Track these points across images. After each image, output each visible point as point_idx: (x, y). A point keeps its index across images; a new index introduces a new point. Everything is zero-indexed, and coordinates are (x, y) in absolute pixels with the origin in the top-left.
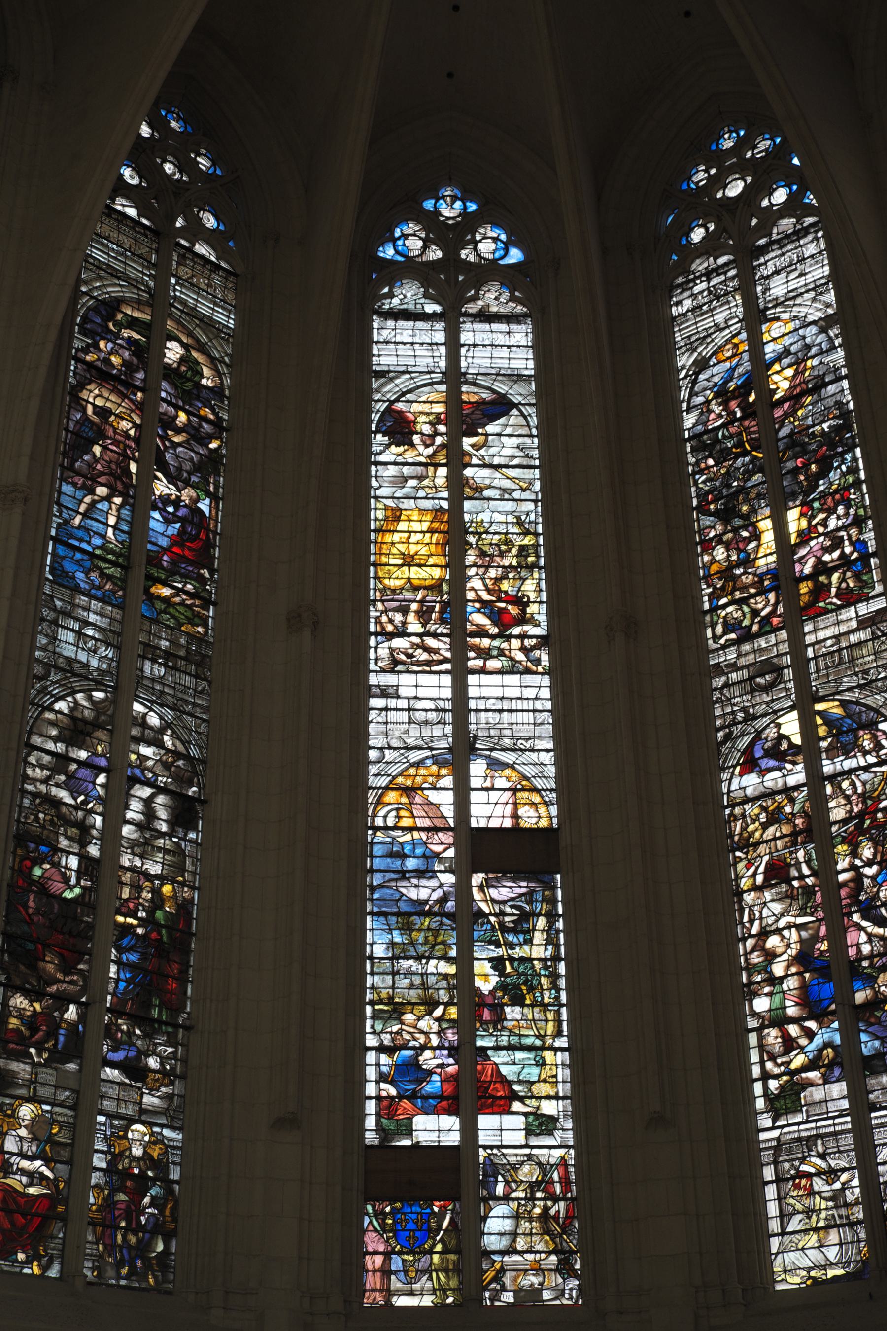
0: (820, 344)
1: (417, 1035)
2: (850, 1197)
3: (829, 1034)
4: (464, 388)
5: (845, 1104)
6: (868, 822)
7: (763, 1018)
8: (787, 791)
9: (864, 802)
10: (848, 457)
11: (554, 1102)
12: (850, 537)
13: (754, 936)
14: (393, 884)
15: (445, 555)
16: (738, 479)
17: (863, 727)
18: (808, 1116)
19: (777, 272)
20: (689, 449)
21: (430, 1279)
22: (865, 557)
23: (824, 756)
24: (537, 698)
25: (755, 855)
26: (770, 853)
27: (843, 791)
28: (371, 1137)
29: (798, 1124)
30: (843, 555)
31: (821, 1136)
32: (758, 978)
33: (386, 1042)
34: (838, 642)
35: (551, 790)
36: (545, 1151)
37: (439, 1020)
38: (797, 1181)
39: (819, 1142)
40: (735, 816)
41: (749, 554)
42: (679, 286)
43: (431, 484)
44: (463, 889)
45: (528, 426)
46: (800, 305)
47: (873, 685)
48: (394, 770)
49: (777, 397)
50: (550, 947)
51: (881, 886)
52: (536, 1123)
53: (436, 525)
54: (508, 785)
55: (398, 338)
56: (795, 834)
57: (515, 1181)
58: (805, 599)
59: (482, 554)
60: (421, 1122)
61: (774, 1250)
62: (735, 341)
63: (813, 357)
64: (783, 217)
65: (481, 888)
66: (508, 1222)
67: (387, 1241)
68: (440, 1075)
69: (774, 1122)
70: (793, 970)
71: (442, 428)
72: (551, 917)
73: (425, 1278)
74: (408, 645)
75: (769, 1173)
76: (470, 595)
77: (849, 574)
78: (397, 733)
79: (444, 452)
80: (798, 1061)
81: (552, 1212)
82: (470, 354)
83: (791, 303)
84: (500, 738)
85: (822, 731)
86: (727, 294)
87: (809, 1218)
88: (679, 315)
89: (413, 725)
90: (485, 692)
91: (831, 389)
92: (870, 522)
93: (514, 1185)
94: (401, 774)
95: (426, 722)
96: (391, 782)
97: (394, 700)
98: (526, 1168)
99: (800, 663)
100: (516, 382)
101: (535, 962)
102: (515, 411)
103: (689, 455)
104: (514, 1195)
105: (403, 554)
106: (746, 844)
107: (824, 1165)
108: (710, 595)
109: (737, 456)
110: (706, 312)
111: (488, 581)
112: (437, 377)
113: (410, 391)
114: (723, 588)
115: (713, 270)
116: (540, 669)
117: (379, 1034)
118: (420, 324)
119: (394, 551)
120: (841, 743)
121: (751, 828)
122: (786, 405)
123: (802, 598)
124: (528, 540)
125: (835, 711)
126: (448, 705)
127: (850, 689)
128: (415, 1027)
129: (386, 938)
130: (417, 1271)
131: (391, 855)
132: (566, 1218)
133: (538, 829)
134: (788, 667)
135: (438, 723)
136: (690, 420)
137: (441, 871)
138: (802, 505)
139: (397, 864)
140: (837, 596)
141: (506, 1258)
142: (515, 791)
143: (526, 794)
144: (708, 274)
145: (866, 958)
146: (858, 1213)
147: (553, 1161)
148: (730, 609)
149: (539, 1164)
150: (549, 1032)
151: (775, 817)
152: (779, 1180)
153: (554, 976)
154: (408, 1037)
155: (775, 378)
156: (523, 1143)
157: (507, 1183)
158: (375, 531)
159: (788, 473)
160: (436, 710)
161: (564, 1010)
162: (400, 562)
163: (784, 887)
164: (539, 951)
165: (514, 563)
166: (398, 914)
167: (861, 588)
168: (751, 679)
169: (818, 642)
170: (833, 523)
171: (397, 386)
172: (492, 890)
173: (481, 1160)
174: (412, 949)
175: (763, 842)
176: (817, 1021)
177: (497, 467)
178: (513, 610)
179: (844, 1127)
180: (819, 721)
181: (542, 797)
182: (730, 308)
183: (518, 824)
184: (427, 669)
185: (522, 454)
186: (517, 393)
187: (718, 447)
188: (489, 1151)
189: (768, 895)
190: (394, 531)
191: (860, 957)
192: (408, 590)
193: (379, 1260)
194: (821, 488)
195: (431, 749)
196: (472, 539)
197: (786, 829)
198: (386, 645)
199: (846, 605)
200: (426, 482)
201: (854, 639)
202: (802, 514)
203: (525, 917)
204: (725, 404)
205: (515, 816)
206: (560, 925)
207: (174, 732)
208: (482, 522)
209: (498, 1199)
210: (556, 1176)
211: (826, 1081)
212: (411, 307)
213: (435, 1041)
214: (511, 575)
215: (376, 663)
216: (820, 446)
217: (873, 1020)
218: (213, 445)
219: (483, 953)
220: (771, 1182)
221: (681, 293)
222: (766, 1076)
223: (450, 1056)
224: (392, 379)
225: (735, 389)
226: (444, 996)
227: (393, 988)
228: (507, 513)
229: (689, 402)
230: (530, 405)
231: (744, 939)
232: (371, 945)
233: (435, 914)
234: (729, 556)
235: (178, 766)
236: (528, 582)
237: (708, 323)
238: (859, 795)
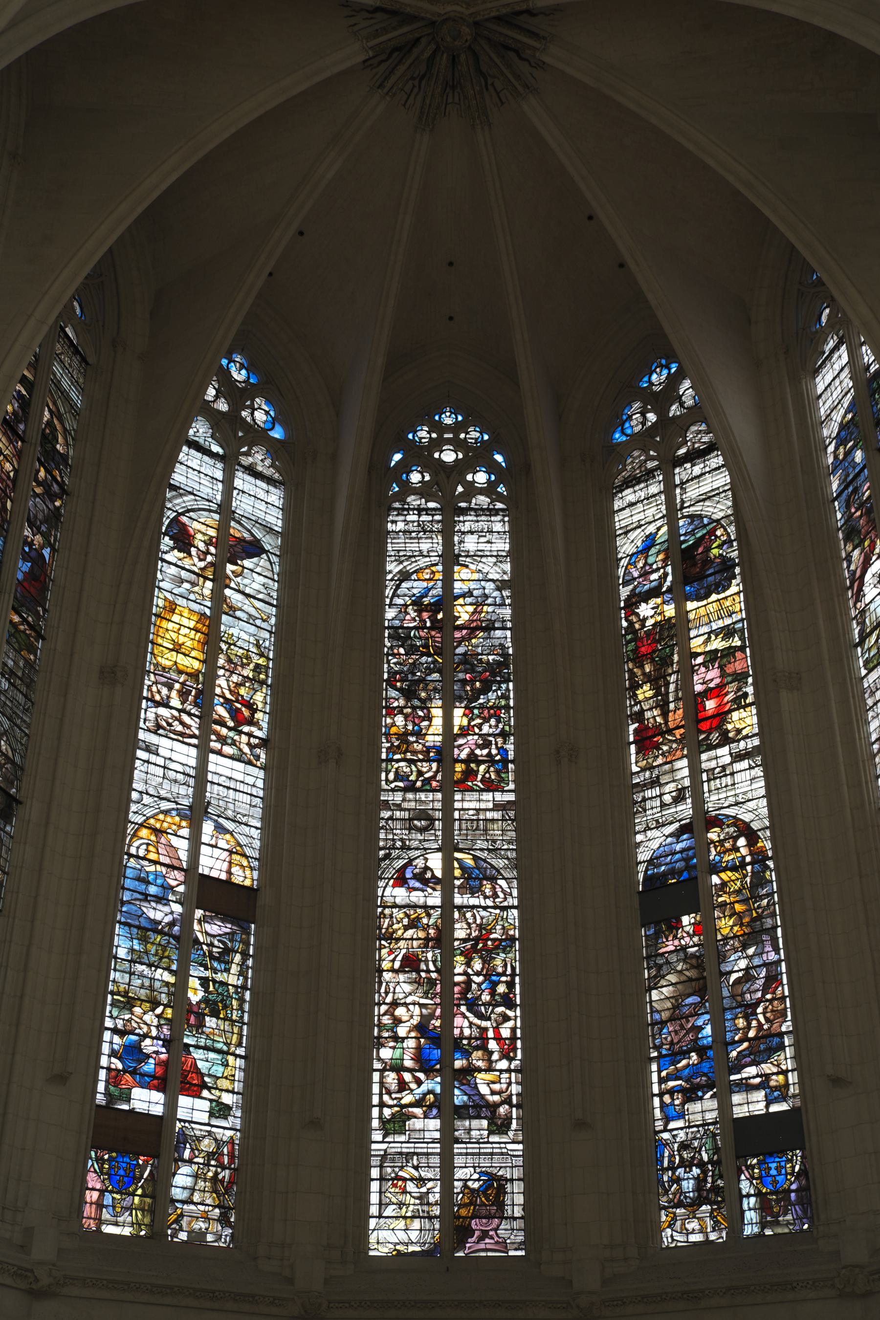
1: (142, 1026)
2: (432, 1199)
3: (434, 1084)
4: (233, 524)
5: (437, 1135)
6: (481, 945)
7: (386, 1063)
8: (425, 907)
9: (480, 931)
10: (504, 686)
11: (231, 1095)
12: (496, 744)
13: (387, 1004)
14: (138, 903)
15: (203, 653)
16: (421, 672)
17: (487, 879)
18: (409, 1138)
19: (472, 533)
20: (386, 635)
21: (131, 1215)
22: (505, 761)
23: (456, 890)
24: (254, 786)
25: (396, 946)
26: (408, 948)
27: (466, 920)
28: (100, 1099)
29: (402, 1143)
30: (490, 753)
31: (418, 1154)
32: (386, 1034)
33: (119, 1026)
34: (478, 814)
35: (255, 859)
36: (221, 1130)
37: (159, 1016)
39: (415, 1158)
40: (385, 915)
41: (422, 729)
43: (200, 592)
44: (186, 920)
45: (272, 571)
48: (149, 812)
49: (458, 623)
50: (241, 978)
51: (483, 991)
52: (217, 1109)
53: (199, 626)
54: (227, 847)
55: (189, 463)
56: (427, 939)
57: (198, 1150)
58: (458, 776)
59: (229, 661)
60: (138, 1093)
61: (372, 1227)
62: (433, 569)
63: (489, 605)
64: (481, 494)
65: (200, 921)
66: (190, 1179)
67: (103, 1182)
68: (155, 1059)
69: (384, 1137)
70: (413, 1034)
71: (212, 550)
72: (245, 955)
73: (127, 1213)
74: (169, 716)
75: (375, 1173)
76: (218, 691)
77: (492, 769)
78: (154, 783)
79: (212, 569)
80: (407, 1099)
81: (220, 1177)
82: (239, 498)
83: (479, 559)
84: (225, 809)
85: (457, 873)
86: (431, 531)
87: (401, 1209)
88: (393, 531)
89: (165, 781)
90: (220, 770)
91: (498, 633)
92: (512, 738)
93: (196, 1152)
94: (153, 817)
95: (176, 781)
96: (145, 821)
97: (154, 756)
98: (206, 1141)
99: (448, 820)
100: (268, 533)
101: (230, 987)
102: (264, 556)
103: (386, 640)
104: (196, 1160)
105: (174, 641)
106: (390, 937)
107: (416, 1174)
108: (388, 749)
109: (422, 655)
110: (414, 538)
111: (231, 683)
112: (214, 507)
113: (193, 510)
114: (398, 747)
115: (424, 509)
116: (258, 764)
117: (115, 1019)
118: (206, 458)
119: (168, 636)
121: (395, 927)
122: (464, 632)
123: (456, 774)
124: (262, 661)
126: (192, 772)
127: (482, 850)
128: (141, 1019)
129: (128, 944)
130: (122, 1208)
131: (139, 879)
132: (229, 1182)
133: (243, 886)
134: (439, 820)
135: (184, 784)
136: (390, 614)
137: (173, 901)
138: (466, 707)
139: (142, 887)
140: (481, 781)
141: (185, 1207)
142: (231, 852)
143: (238, 857)
144: (420, 511)
145: (466, 1038)
146: (436, 1211)
147: (225, 1139)
149: (216, 1140)
150: (233, 1042)
151: (413, 924)
152: (382, 1179)
153: (241, 1000)
154: (135, 1025)
156: (207, 1122)
157: (192, 1150)
158: (155, 615)
159: (459, 681)
160: (184, 773)
161: (245, 1027)
162: (171, 647)
163: (414, 975)
164: (233, 980)
165: (251, 676)
166: (139, 927)
167: (499, 782)
168: (410, 820)
169: (463, 809)
170: (486, 729)
171: (184, 502)
172: (206, 925)
173: (177, 1129)
174: (146, 957)
175: (403, 939)
176: (425, 1074)
177: (248, 596)
178: (246, 712)
180: (456, 865)
181: (249, 862)
183: (231, 879)
184: (181, 739)
185: (265, 592)
186: (269, 543)
188: (182, 1124)
189: (402, 977)
190: (169, 620)
191: (462, 1037)
192: (174, 672)
193: (95, 1195)
194: (481, 701)
195: (177, 803)
196: (224, 647)
197: (421, 934)
198: (154, 710)
200: (196, 589)
201: (489, 815)
202: (464, 715)
203: (227, 951)
204: (419, 612)
205: (229, 872)
206: (250, 962)
207: (8, 739)
208: (232, 635)
209: (185, 1161)
210: (225, 1151)
211: (426, 1117)
212: (201, 441)
213: (154, 1032)
214: (247, 684)
215: (145, 723)
216: (485, 671)
217: (465, 1082)
218: (57, 504)
219: (197, 971)
220: (377, 1179)
221: (397, 515)
223: (163, 1046)
224: (181, 495)
225: (427, 605)
226: (164, 999)
227: (129, 984)
228: (250, 635)
230: (275, 555)
231: (379, 1004)
232: (117, 947)
233: (166, 934)
234: (406, 725)
235: (6, 768)
236: (259, 693)
237: (414, 546)
238: (477, 925)
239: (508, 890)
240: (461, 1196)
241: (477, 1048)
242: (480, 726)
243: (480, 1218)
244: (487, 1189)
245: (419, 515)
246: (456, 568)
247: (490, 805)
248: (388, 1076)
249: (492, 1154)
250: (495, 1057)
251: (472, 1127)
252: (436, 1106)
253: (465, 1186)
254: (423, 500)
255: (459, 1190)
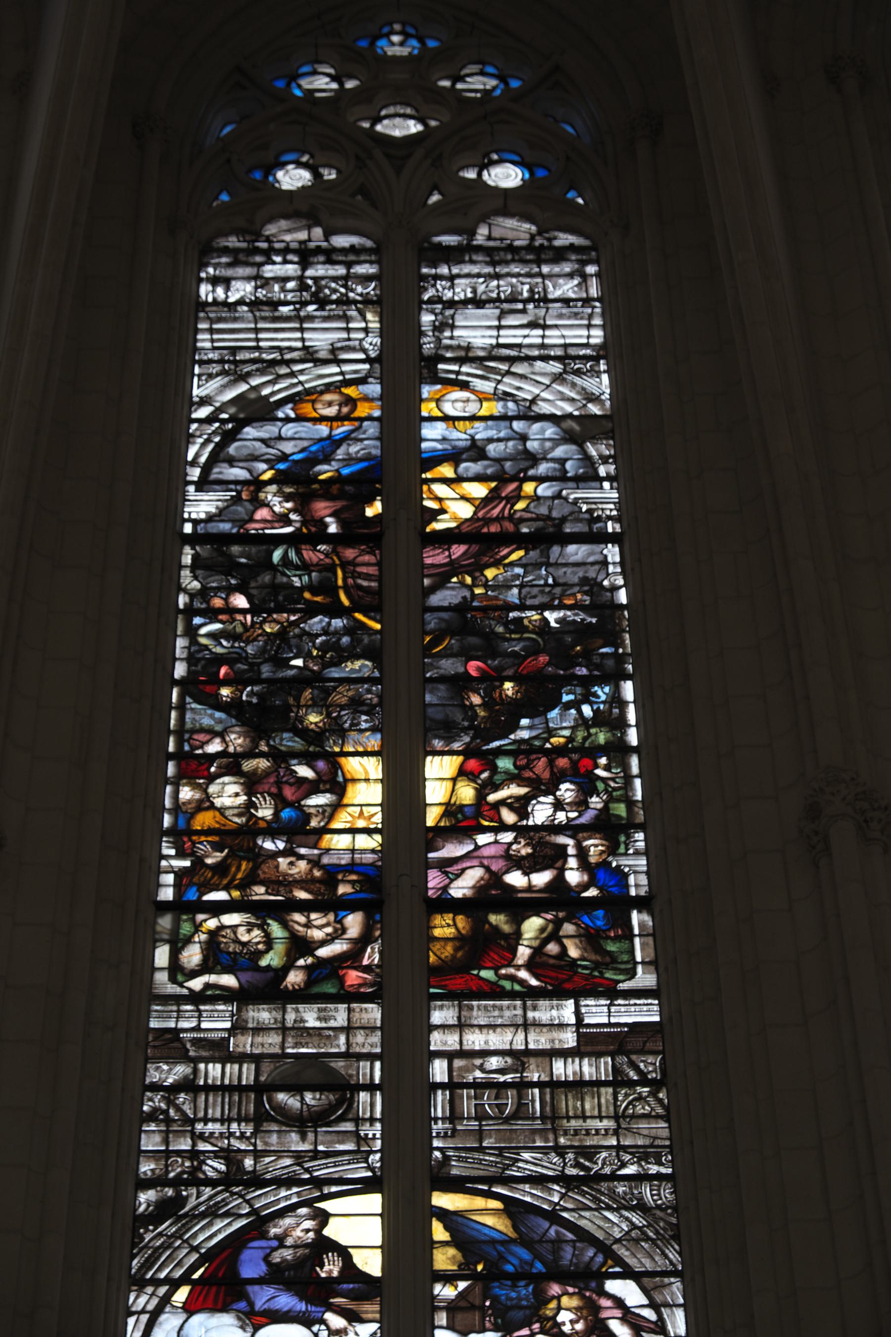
0: (562, 461)
10: (602, 693)
12: (582, 854)
16: (307, 656)
17: (564, 1277)
19: (478, 303)
20: (187, 559)
23: (442, 1318)
30: (559, 881)
41: (308, 817)
42: (226, 251)
46: (523, 377)
47: (604, 1186)
62: (351, 391)
63: (540, 480)
77: (568, 928)
83: (504, 367)
85: (444, 1259)
86: (344, 301)
88: (215, 302)
91: (576, 552)
92: (640, 836)
103: (186, 573)
108: (180, 874)
109: (311, 611)
110: (287, 319)
114: (221, 869)
115: (318, 250)
120: (495, 1299)
122: (458, 550)
123: (436, 947)
125: (489, 1221)
134: (371, 1088)
136: (201, 506)
138: (467, 753)
140: (530, 966)
148: (230, 919)
155: (440, 490)
159: (442, 679)
167: (597, 966)
168: (260, 1089)
170: (541, 812)
180: (439, 1232)
182: (348, 330)
187: (267, 578)
199: (558, 993)
201: (561, 1069)
202: (462, 772)
204: (303, 502)
216: (533, 650)
229: (207, 469)
234: (250, 805)
237: (289, 339)
239: (649, 1314)
242: (521, 806)
245: (305, 264)
246: (426, 391)
247: (569, 1039)
254: (318, 232)
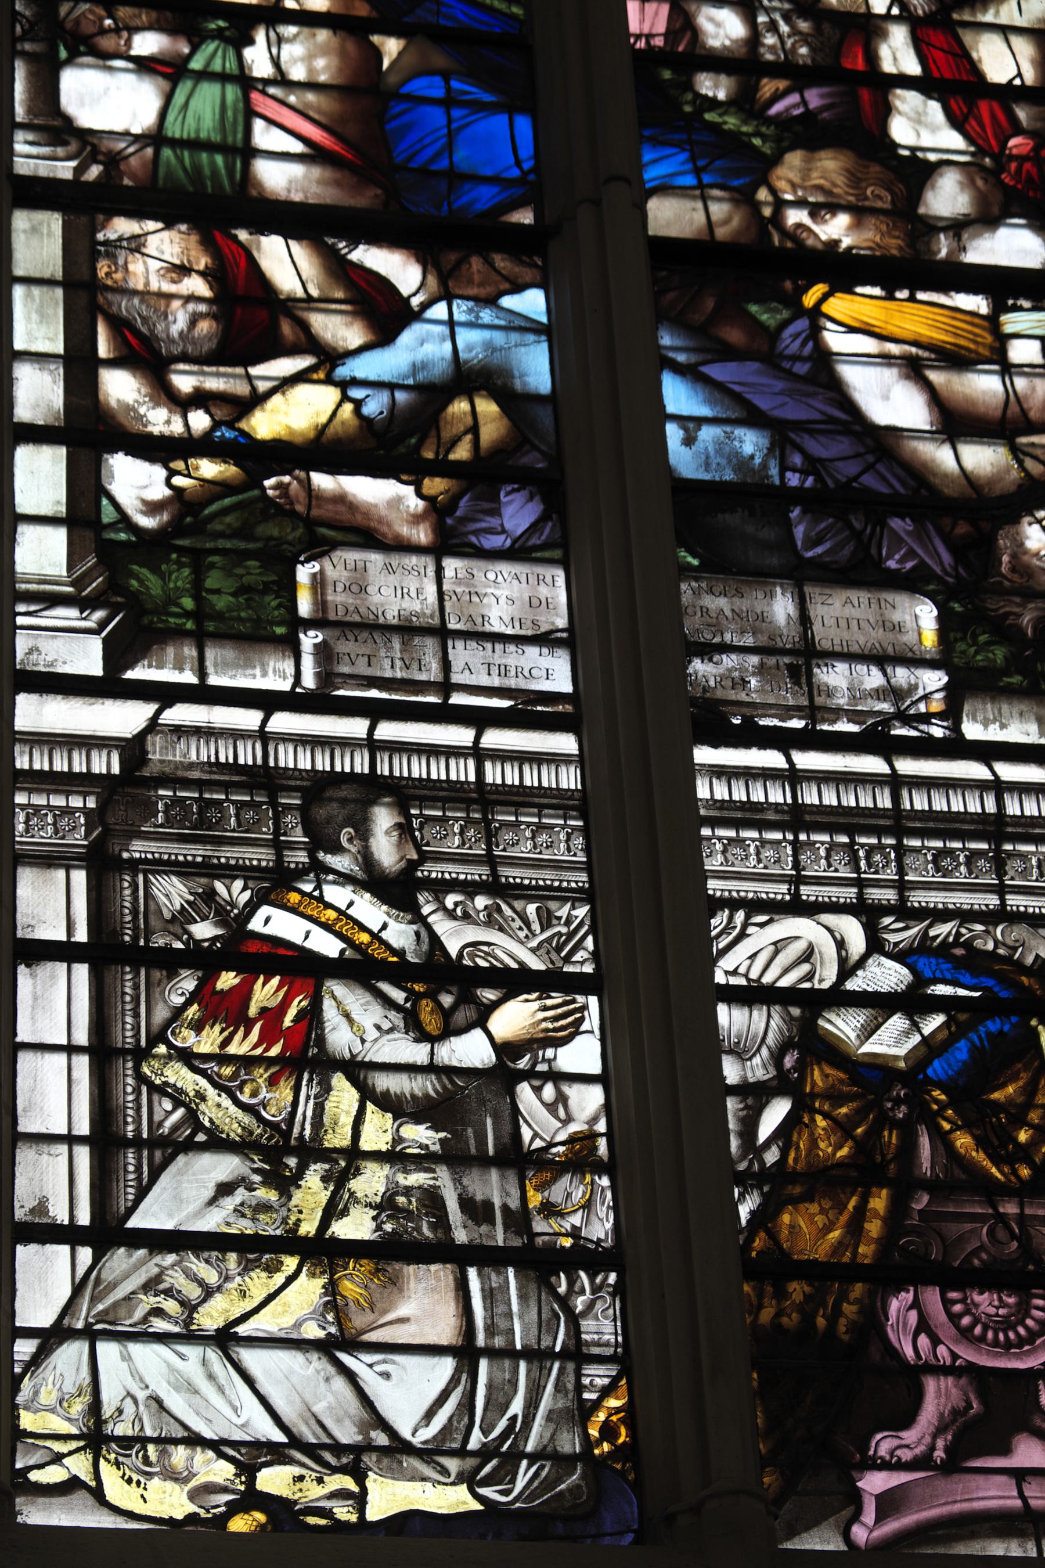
2: (537, 1119)
7: (113, 162)
18: (327, 677)
29: (268, 702)
31: (404, 794)
38: (227, 980)
39: (384, 819)
69: (118, 654)
80: (297, 411)
87: (287, 1184)
107: (400, 934)
176: (426, 258)
179: (548, 777)
217: (734, 335)
222: (89, 434)
240: (775, 1113)
241: (807, 134)
243: (955, 1278)
244: (988, 1067)
248: (136, 244)
249: (996, 828)
250: (947, 198)
251: (825, 634)
252: (526, 480)
253: (808, 1043)
255: (758, 1069)
